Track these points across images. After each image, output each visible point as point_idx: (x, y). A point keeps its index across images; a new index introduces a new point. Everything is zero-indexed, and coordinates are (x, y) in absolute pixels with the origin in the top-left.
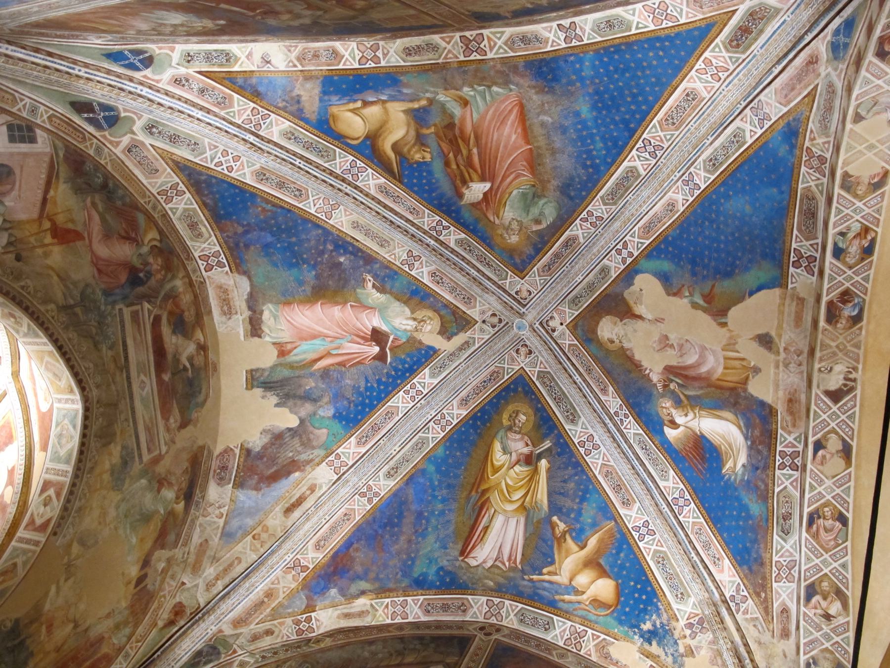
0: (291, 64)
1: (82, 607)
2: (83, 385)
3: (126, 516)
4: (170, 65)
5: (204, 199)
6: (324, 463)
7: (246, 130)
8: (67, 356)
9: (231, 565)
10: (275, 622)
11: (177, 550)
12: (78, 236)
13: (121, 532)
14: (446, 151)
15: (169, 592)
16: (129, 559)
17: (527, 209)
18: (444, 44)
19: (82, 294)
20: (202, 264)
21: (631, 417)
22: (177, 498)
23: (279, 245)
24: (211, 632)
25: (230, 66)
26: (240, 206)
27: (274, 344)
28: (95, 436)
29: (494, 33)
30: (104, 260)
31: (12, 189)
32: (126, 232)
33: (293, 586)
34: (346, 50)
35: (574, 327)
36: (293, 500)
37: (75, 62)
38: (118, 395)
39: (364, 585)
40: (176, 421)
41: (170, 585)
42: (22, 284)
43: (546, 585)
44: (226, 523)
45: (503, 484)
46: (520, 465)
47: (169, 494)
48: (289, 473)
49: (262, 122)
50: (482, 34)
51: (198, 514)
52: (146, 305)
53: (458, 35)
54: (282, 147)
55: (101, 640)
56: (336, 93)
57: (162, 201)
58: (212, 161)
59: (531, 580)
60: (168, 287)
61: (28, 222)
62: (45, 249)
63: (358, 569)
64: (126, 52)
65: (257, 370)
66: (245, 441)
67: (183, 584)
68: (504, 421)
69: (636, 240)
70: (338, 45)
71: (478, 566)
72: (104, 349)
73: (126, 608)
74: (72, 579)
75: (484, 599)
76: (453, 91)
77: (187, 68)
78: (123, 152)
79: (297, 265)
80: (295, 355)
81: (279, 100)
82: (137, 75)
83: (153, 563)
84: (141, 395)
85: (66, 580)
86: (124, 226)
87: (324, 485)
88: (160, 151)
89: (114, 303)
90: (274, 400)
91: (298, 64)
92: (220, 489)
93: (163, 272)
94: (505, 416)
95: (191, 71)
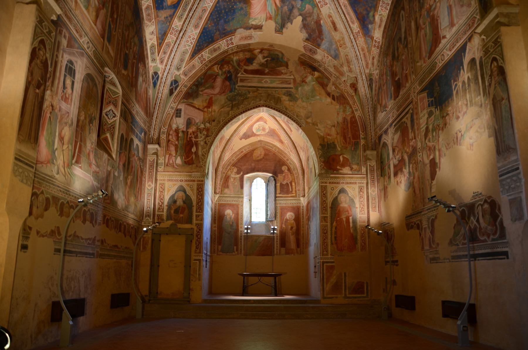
0: (153, 24)
1: (329, 122)
2: (258, 106)
3: (308, 99)
4: (157, 66)
5: (205, 47)
6: (321, 9)
7: (178, 36)
8: (247, 110)
9: (347, 59)
10: (372, 54)
11: (332, 80)
12: (211, 98)
13: (312, 102)
15: (345, 87)
16: (323, 101)
19: (229, 100)
20: (230, 46)
22: (312, 75)
23: (225, 17)
24: (365, 78)
25: (155, 45)
26: (208, 33)
27: (266, 21)
28: (276, 105)
30: (220, 90)
31: (194, 119)
32: (212, 80)
33: (363, 39)
34: (145, 4)
36: (332, 26)
37: (157, 96)
38: (266, 93)
39: (371, 14)
40: (284, 69)
41: (342, 87)
42: (221, 121)
44: (331, 56)
47: (309, 78)
48: (320, 25)
49: (175, 30)
51: (323, 66)
52: (239, 75)
54: (185, 21)
55: (345, 119)
56: (162, 4)
57: (205, 62)
58: (190, 46)
60: (235, 64)
61: (204, 116)
62: (213, 111)
63: (365, 13)
64: (153, 81)
65: (276, 29)
66: (303, 40)
67: (344, 81)
70: (144, 8)
72: (249, 95)
73: (340, 106)
74: (319, 125)
77: (157, 60)
78: (186, 77)
79: (234, 10)
80: (272, 13)
81: (167, 25)
82: (160, 76)
83: (330, 92)
84: (269, 83)
85: (317, 126)
86: (211, 80)
87: (330, 11)
88: (186, 65)
89: (235, 89)
90: (289, 24)
91: (153, 21)
92: (318, 54)
93: (230, 65)
95: (158, 58)
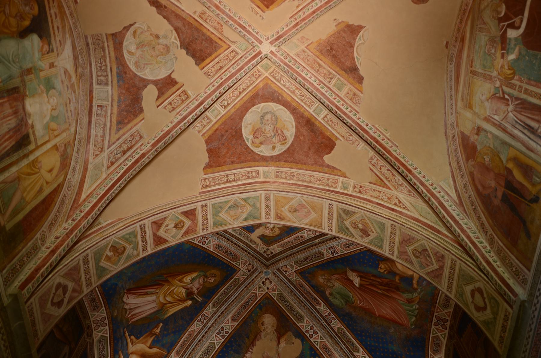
14: (383, 279)
17: (338, 293)
18: (446, 311)
21: (223, 340)
29: (445, 334)
35: (267, 298)
43: (125, 343)
45: (174, 287)
46: (186, 291)
50: (446, 329)
53: (449, 319)
59: (124, 333)
68: (209, 272)
69: (319, 340)
71: (124, 302)
75: (105, 315)
76: (418, 301)
94: (213, 271)
